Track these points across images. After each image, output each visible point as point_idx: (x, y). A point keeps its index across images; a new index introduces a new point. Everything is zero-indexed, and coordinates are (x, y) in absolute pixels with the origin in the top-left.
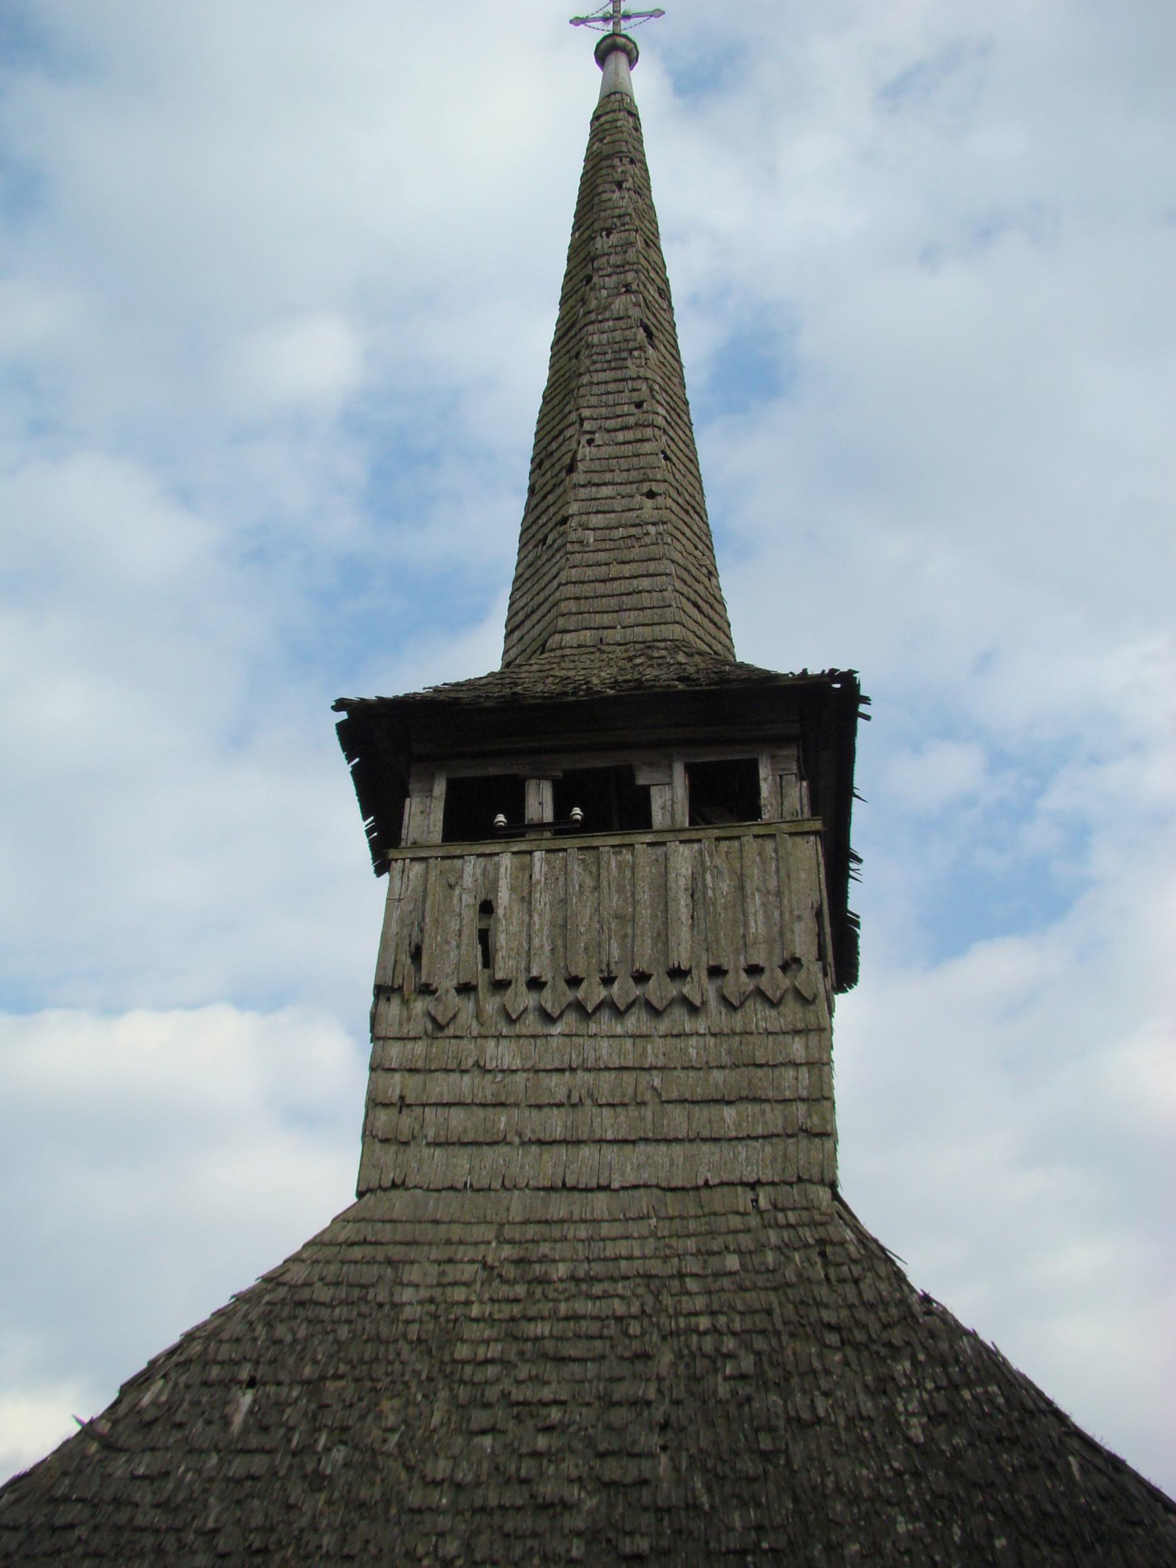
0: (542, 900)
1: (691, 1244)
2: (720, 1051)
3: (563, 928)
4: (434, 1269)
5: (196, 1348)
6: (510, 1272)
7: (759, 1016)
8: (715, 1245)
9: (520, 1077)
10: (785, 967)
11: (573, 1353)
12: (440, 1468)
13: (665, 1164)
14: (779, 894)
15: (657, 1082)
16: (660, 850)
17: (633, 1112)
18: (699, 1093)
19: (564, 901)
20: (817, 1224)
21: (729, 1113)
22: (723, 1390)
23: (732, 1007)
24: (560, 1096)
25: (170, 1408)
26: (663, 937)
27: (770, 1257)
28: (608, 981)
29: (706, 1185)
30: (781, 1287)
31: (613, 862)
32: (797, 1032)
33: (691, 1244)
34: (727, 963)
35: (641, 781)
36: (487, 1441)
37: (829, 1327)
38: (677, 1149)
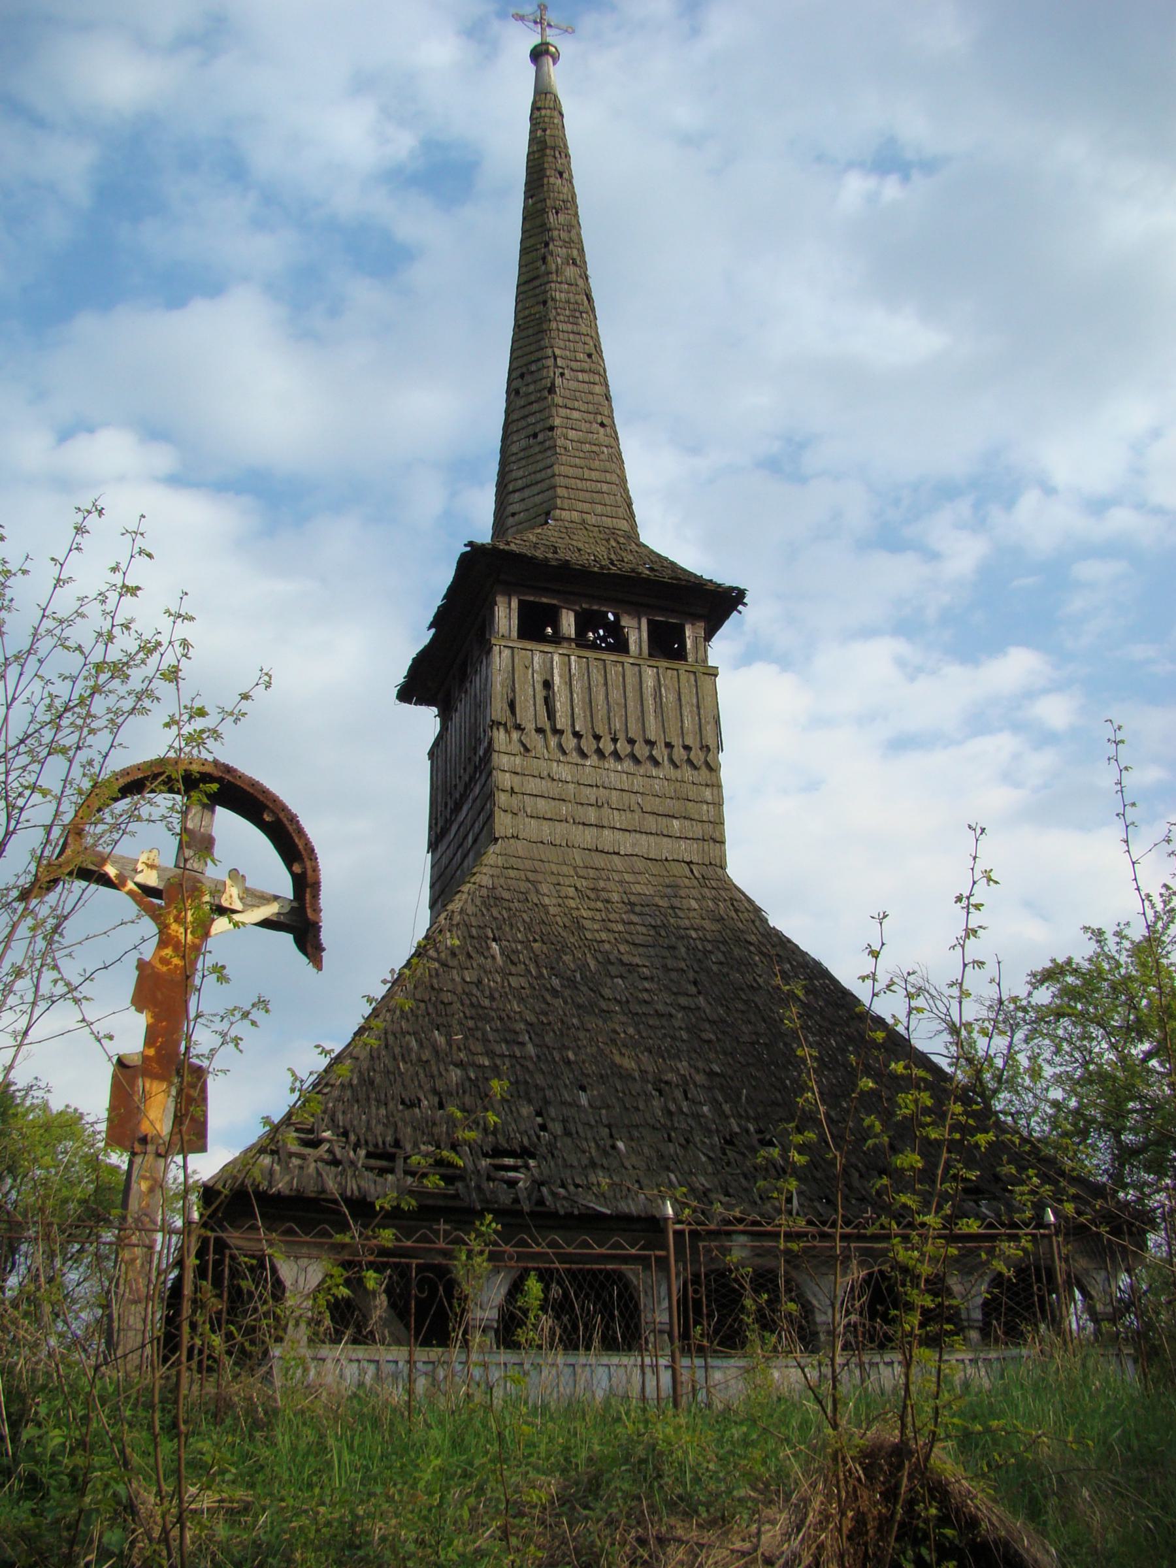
2: (669, 789)
7: (688, 773)
9: (571, 786)
14: (698, 707)
15: (640, 800)
16: (637, 668)
17: (629, 815)
21: (675, 822)
23: (676, 766)
24: (593, 801)
29: (666, 860)
32: (707, 785)
38: (651, 838)
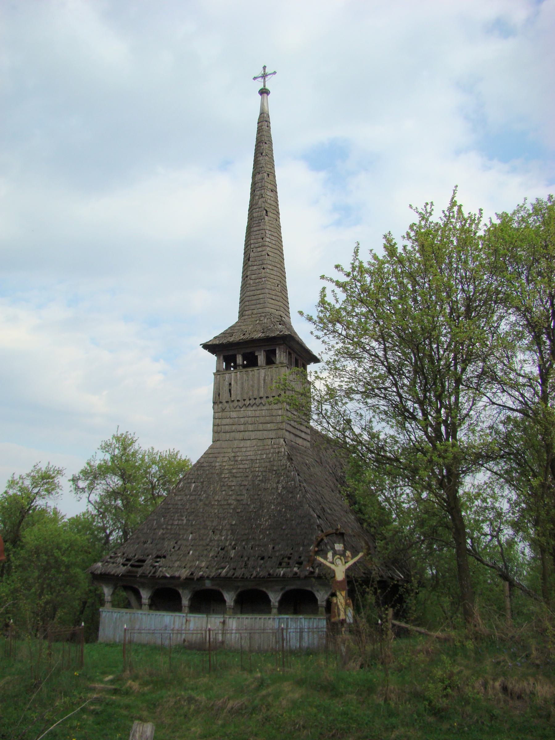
0: (239, 382)
1: (260, 452)
3: (242, 388)
4: (222, 458)
5: (187, 476)
6: (232, 459)
10: (278, 396)
11: (238, 476)
12: (216, 498)
13: (259, 435)
18: (264, 421)
19: (242, 383)
20: (279, 448)
21: (269, 425)
24: (243, 423)
27: (270, 455)
28: (250, 400)
30: (270, 462)
32: (280, 409)
33: (260, 452)
35: (256, 354)
36: (224, 492)
38: (261, 432)
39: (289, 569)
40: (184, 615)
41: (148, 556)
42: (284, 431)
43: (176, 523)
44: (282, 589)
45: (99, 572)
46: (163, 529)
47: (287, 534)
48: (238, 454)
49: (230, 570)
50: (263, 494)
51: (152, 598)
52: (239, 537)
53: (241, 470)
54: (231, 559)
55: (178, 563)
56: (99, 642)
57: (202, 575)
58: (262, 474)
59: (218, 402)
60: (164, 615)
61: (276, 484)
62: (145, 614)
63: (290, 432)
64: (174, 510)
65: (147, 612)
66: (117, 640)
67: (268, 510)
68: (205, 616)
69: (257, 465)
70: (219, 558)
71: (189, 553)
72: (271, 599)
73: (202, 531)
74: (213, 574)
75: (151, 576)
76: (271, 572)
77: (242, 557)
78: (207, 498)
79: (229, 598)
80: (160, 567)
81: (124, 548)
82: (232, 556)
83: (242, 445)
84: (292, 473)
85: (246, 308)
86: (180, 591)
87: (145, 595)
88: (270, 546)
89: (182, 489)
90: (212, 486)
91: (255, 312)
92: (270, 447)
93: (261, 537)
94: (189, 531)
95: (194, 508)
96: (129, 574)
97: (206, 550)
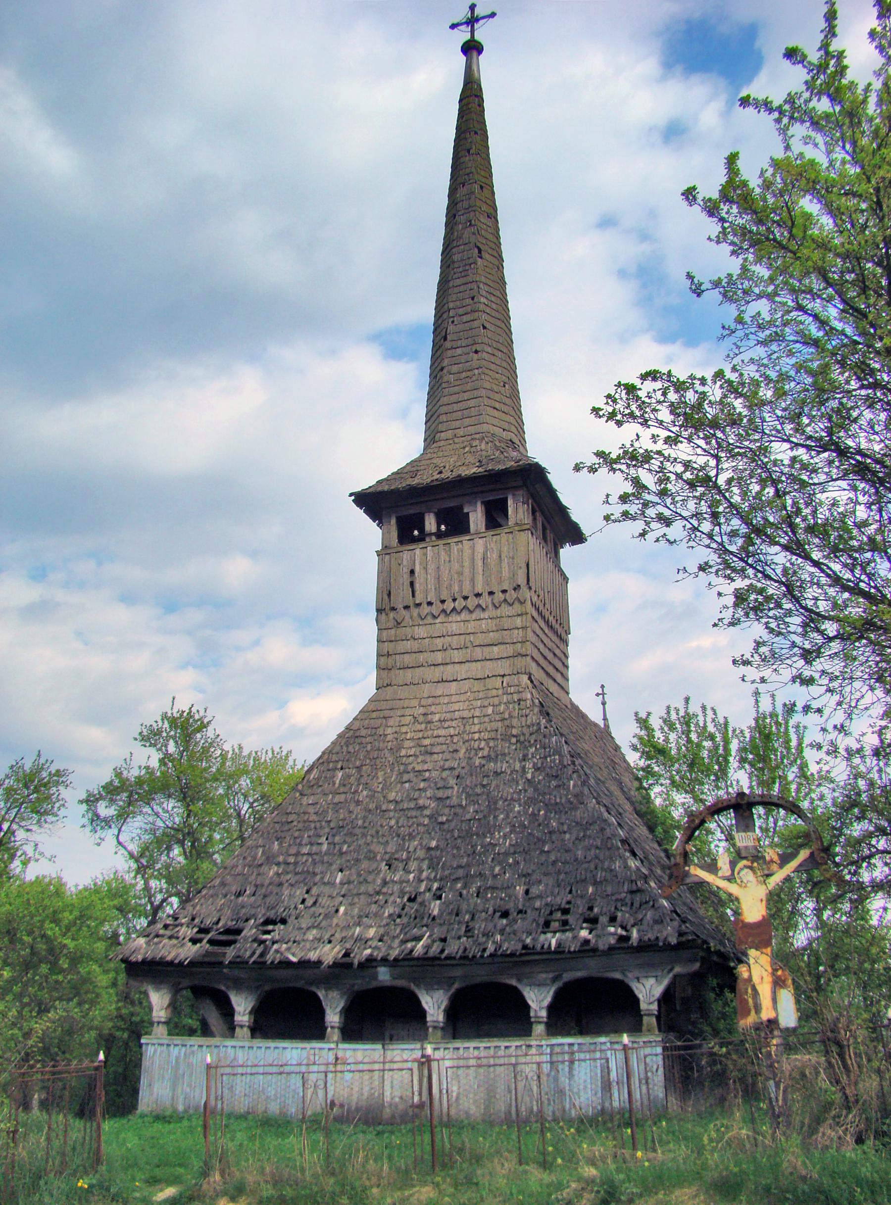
0: (431, 567)
1: (479, 703)
2: (492, 624)
5: (326, 757)
6: (421, 719)
7: (505, 610)
8: (486, 703)
10: (515, 589)
12: (392, 796)
13: (476, 669)
17: (464, 651)
18: (486, 642)
20: (520, 692)
21: (495, 649)
22: (477, 763)
23: (496, 608)
24: (440, 647)
25: (318, 779)
26: (473, 580)
27: (502, 707)
28: (454, 600)
30: (503, 719)
31: (455, 548)
33: (479, 703)
34: (494, 589)
35: (465, 511)
36: (407, 785)
37: (514, 736)
39: (569, 935)
40: (333, 1046)
41: (247, 920)
42: (529, 658)
43: (305, 850)
44: (555, 980)
45: (140, 958)
46: (278, 864)
47: (554, 863)
48: (433, 708)
49: (434, 941)
50: (494, 783)
51: (256, 1012)
52: (447, 872)
53: (442, 740)
54: (434, 919)
55: (312, 934)
56: (139, 1112)
57: (371, 955)
58: (488, 744)
59: (388, 608)
60: (284, 1048)
61: (520, 762)
62: (243, 1047)
63: (538, 664)
64: (300, 826)
65: (247, 1044)
66: (181, 1108)
67: (507, 816)
68: (379, 1046)
69: (476, 728)
70: (405, 920)
71: (337, 911)
72: (530, 1002)
73: (365, 865)
74: (394, 954)
75: (254, 962)
76: (528, 941)
77: (457, 915)
78: (372, 797)
79: (434, 1005)
80: (274, 943)
81: (194, 907)
82: (436, 912)
83: (439, 693)
84: (554, 739)
85: (441, 428)
86: (321, 994)
87: (243, 1006)
88: (520, 890)
89: (317, 783)
90: (380, 774)
91: (460, 432)
92: (500, 692)
93: (497, 869)
94: (334, 867)
95: (344, 819)
96: (206, 959)
97: (376, 902)
